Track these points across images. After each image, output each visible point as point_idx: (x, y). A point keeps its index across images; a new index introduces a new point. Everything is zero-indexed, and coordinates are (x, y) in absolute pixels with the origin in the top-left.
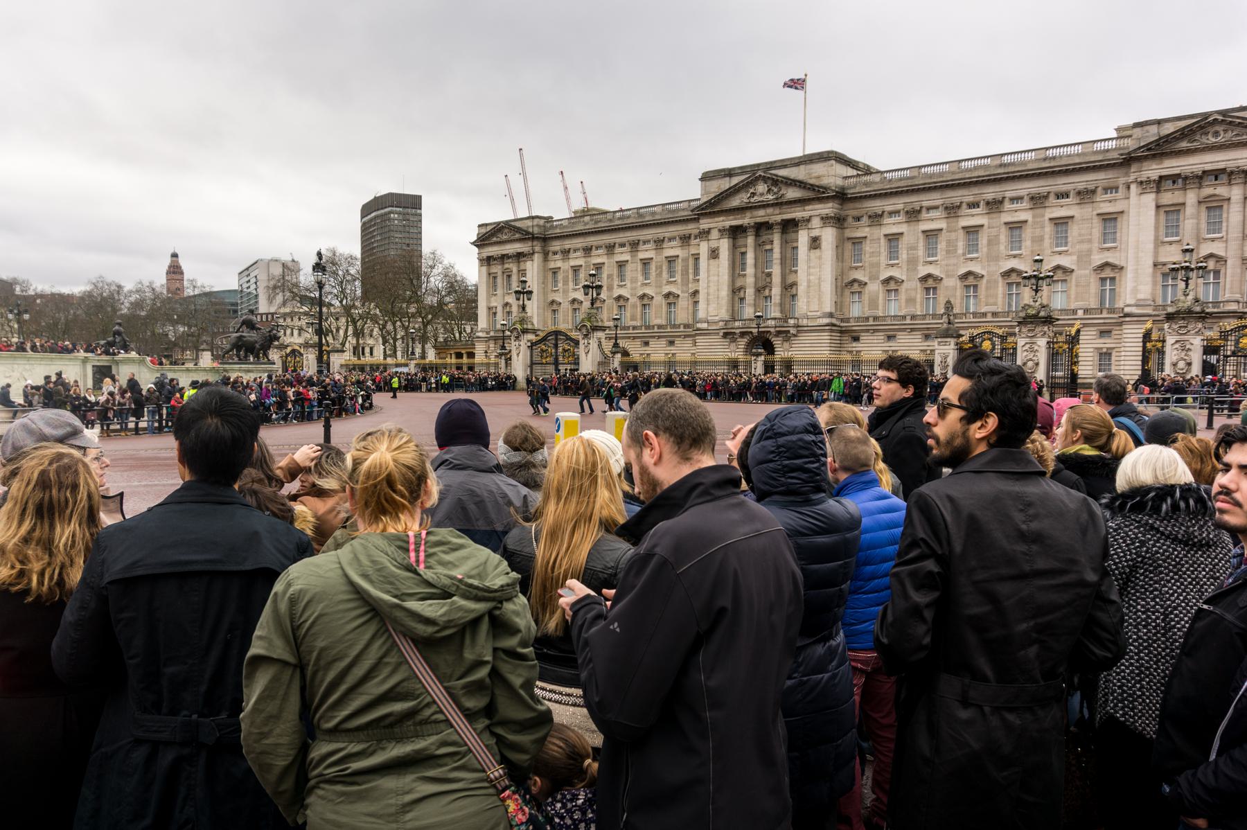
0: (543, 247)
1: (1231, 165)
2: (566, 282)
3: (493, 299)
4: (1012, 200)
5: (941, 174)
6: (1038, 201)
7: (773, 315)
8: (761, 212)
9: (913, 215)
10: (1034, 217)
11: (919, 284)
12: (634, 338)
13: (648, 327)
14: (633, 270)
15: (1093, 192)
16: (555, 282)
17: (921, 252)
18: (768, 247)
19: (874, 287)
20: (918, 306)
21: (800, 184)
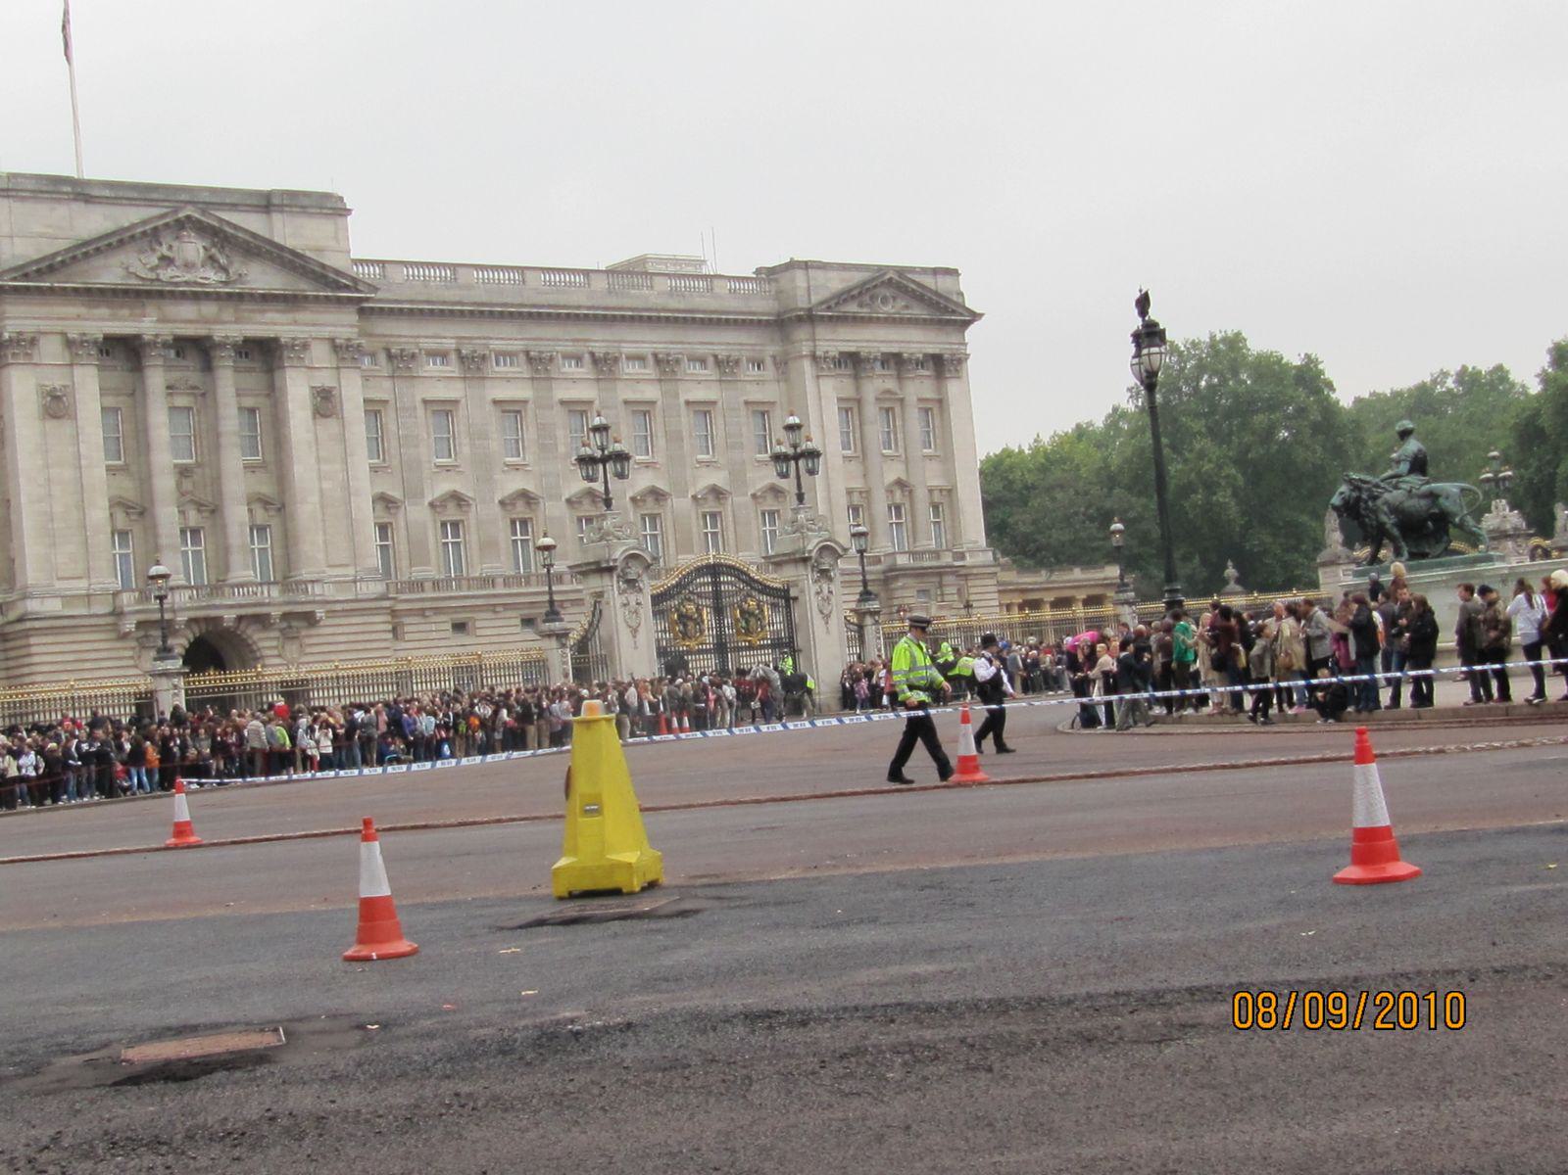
4: (631, 358)
6: (666, 366)
8: (187, 310)
9: (472, 364)
15: (737, 362)
17: (495, 445)
18: (182, 401)
21: (292, 261)
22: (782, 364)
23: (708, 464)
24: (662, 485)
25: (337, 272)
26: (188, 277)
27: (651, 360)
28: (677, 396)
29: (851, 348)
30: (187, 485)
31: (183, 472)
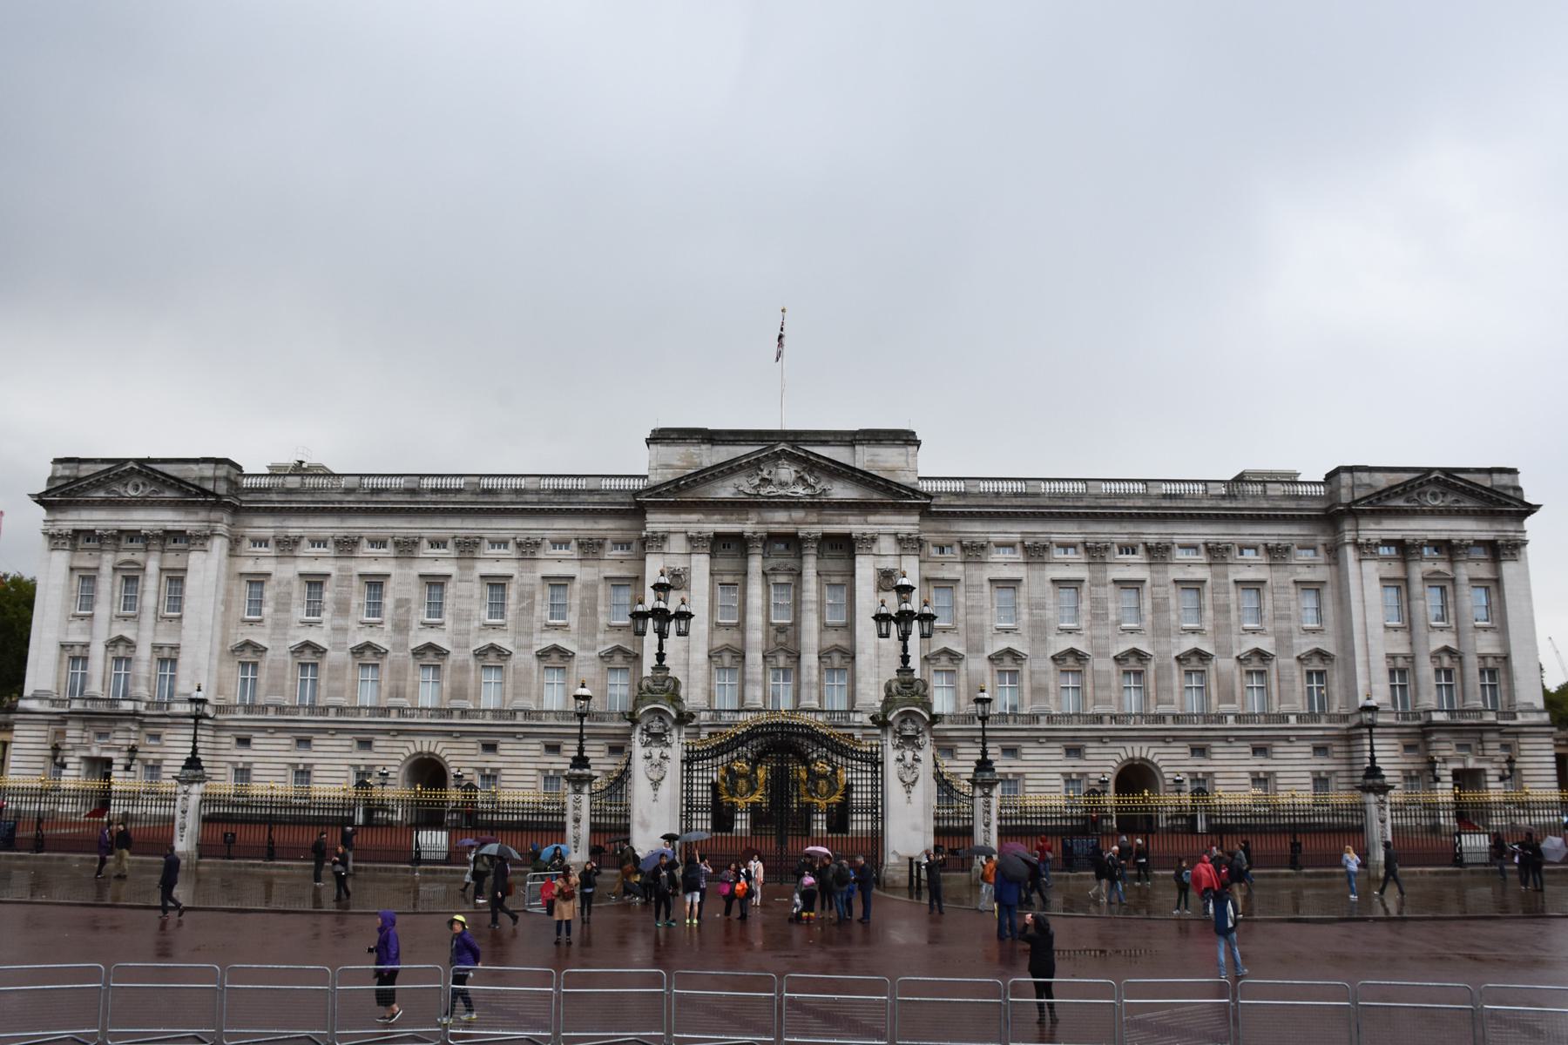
0: (232, 525)
1: (1455, 537)
2: (283, 605)
3: (78, 624)
4: (1182, 547)
5: (1079, 496)
6: (1217, 553)
7: (804, 703)
8: (781, 516)
9: (1035, 553)
10: (1214, 575)
11: (1051, 665)
12: (463, 734)
13: (498, 713)
14: (466, 594)
15: (1287, 549)
16: (256, 604)
18: (782, 579)
19: (978, 666)
20: (1052, 701)
22: (1334, 553)
23: (1254, 631)
24: (1207, 648)
25: (899, 485)
26: (782, 492)
27: (1202, 548)
28: (1226, 577)
29: (1397, 536)
30: (782, 638)
31: (781, 629)
